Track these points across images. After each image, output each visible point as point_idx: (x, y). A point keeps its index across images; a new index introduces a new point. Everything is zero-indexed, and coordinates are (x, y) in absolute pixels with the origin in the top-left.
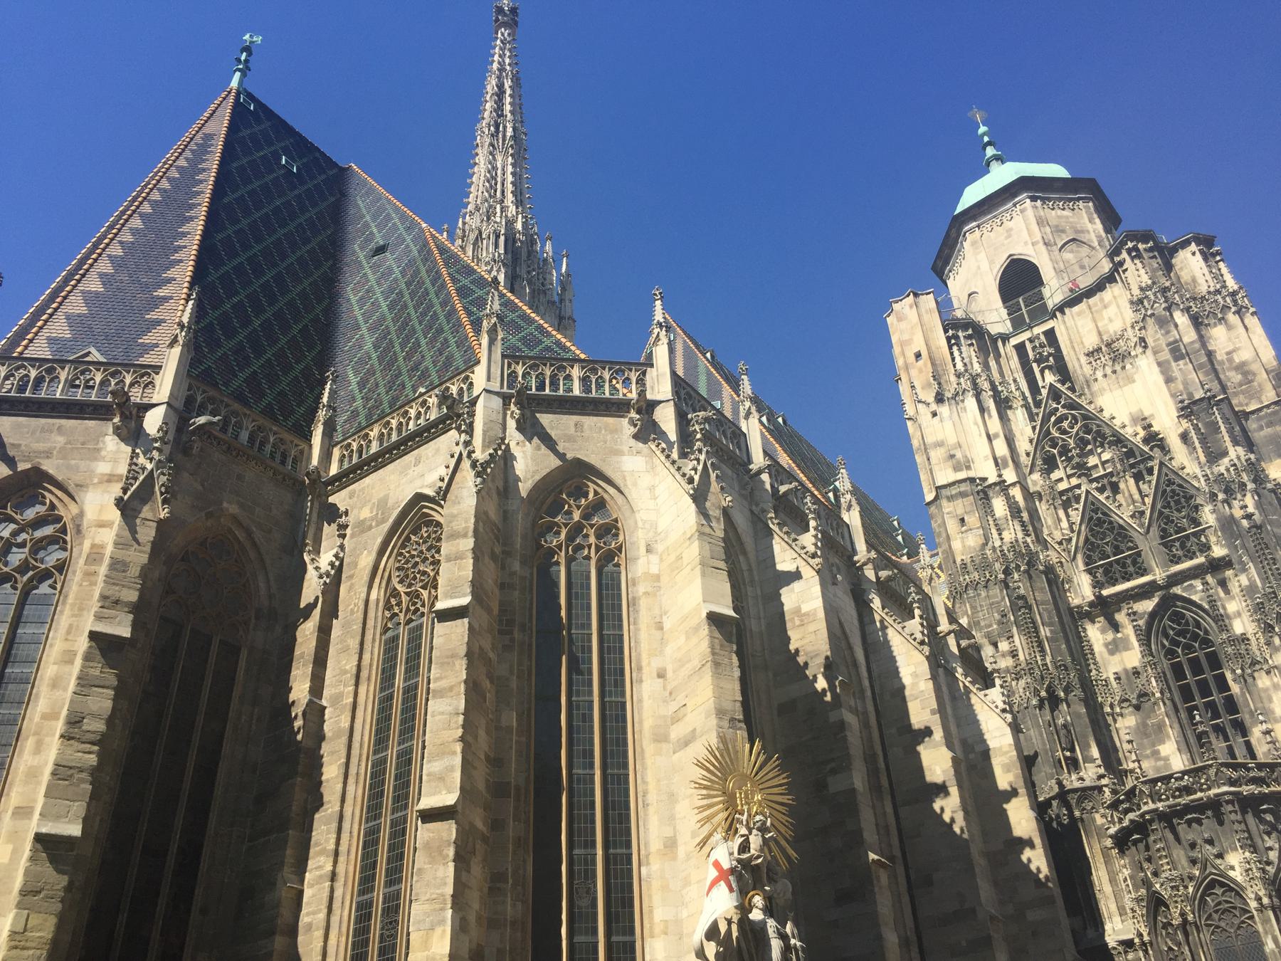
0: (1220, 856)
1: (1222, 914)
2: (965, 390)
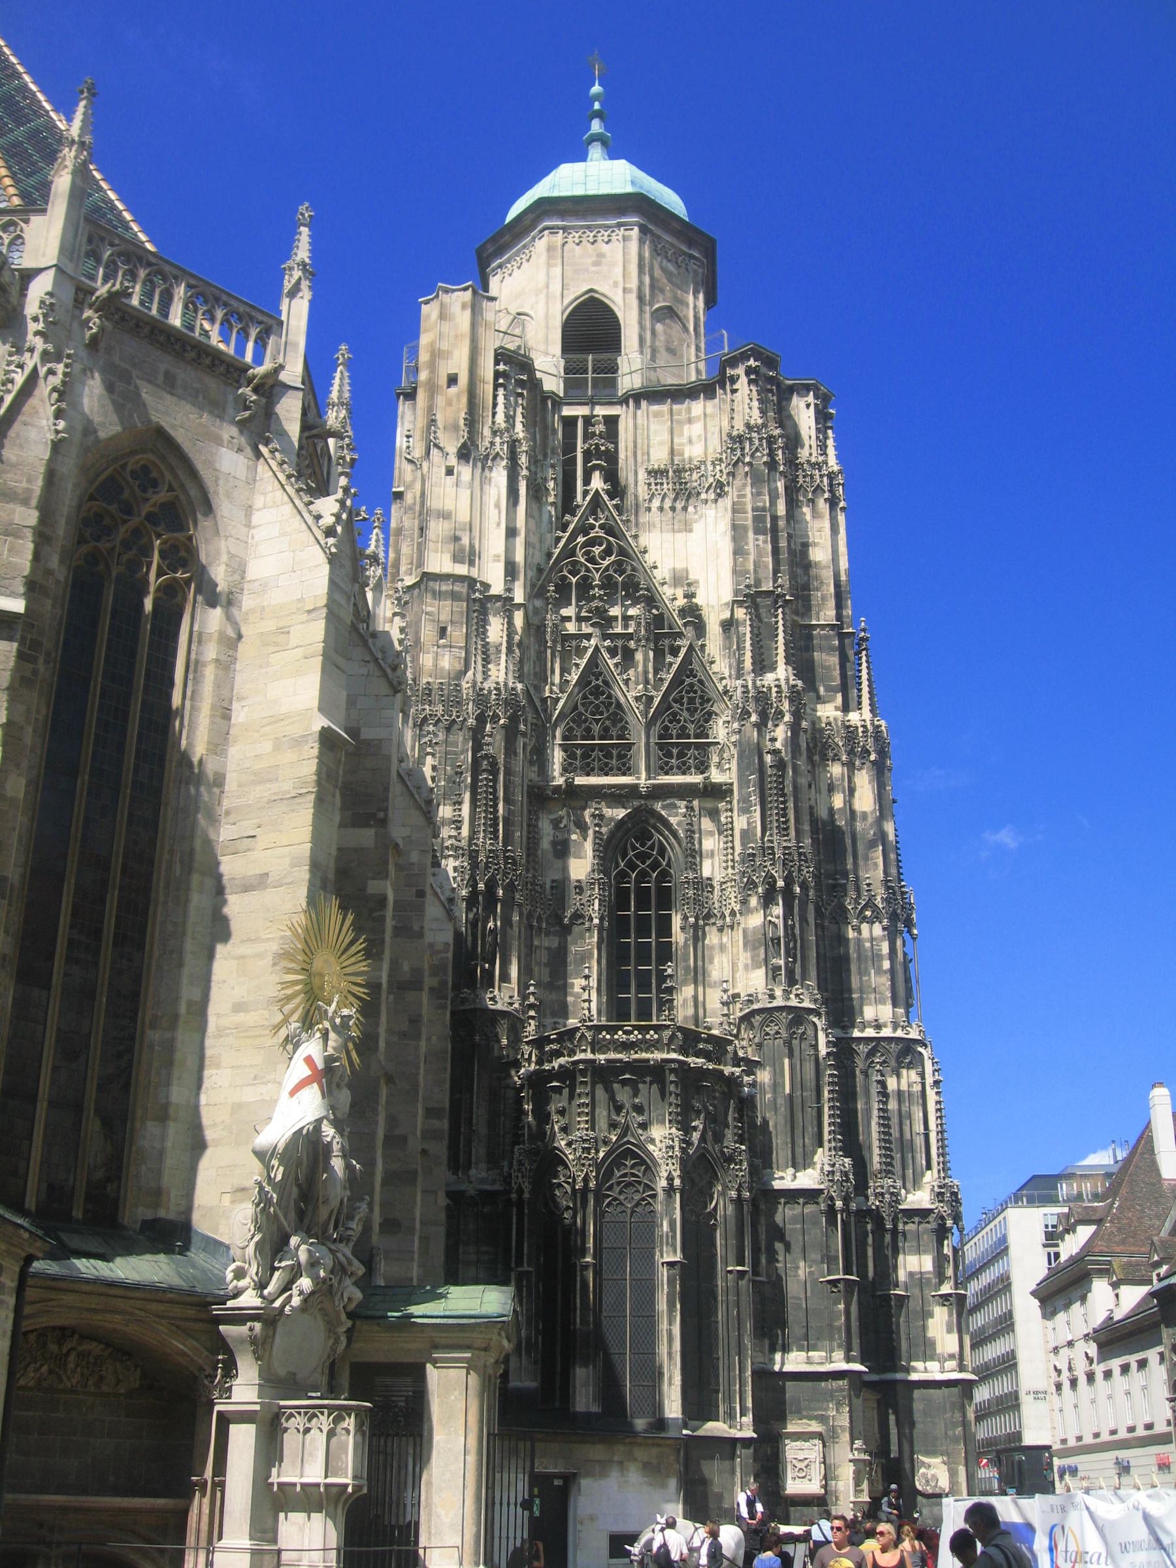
0: (644, 1126)
1: (625, 1187)
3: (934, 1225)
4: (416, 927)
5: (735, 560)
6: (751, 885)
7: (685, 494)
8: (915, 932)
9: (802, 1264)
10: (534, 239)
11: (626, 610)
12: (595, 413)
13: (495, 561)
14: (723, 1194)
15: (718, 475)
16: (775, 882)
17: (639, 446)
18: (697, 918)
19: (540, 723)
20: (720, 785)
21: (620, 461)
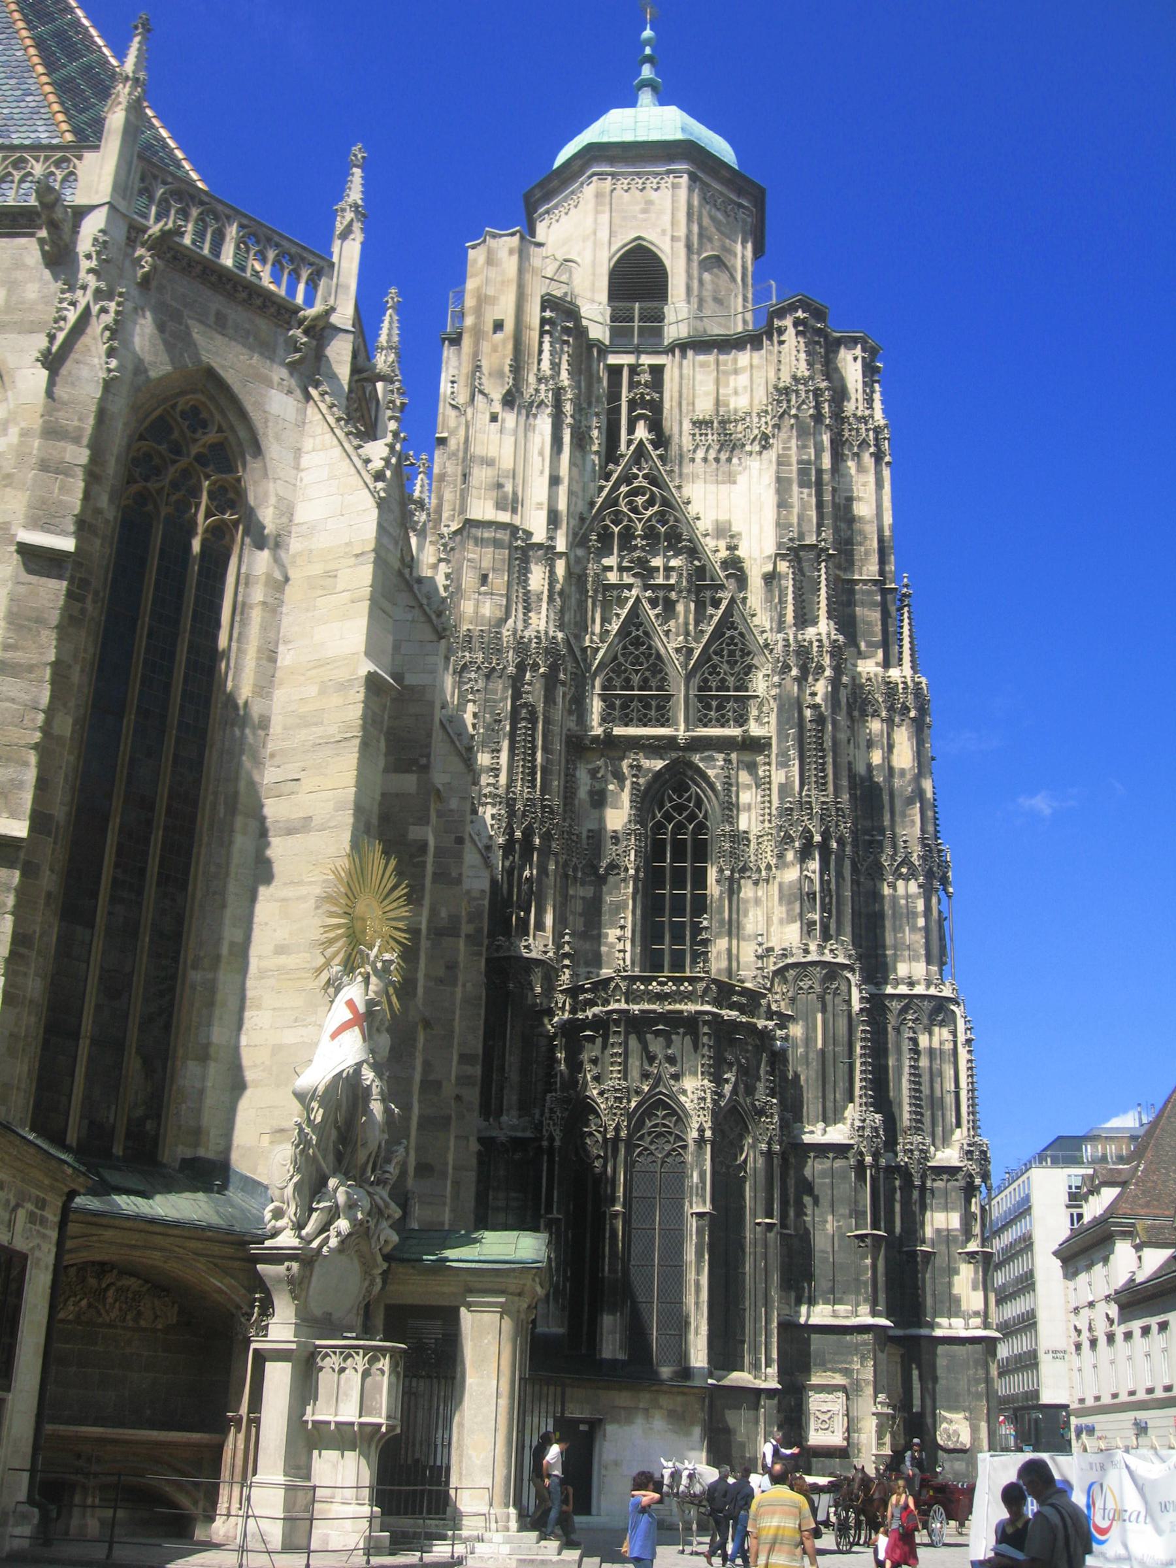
0: (676, 1077)
1: (656, 1137)
2: (542, 402)
3: (962, 1183)
4: (454, 874)
5: (779, 513)
6: (788, 839)
7: (730, 445)
8: (951, 890)
9: (830, 1218)
10: (582, 184)
11: (668, 561)
12: (641, 362)
14: (753, 1146)
15: (762, 429)
16: (812, 837)
17: (684, 396)
18: (732, 871)
20: (759, 738)
21: (665, 412)
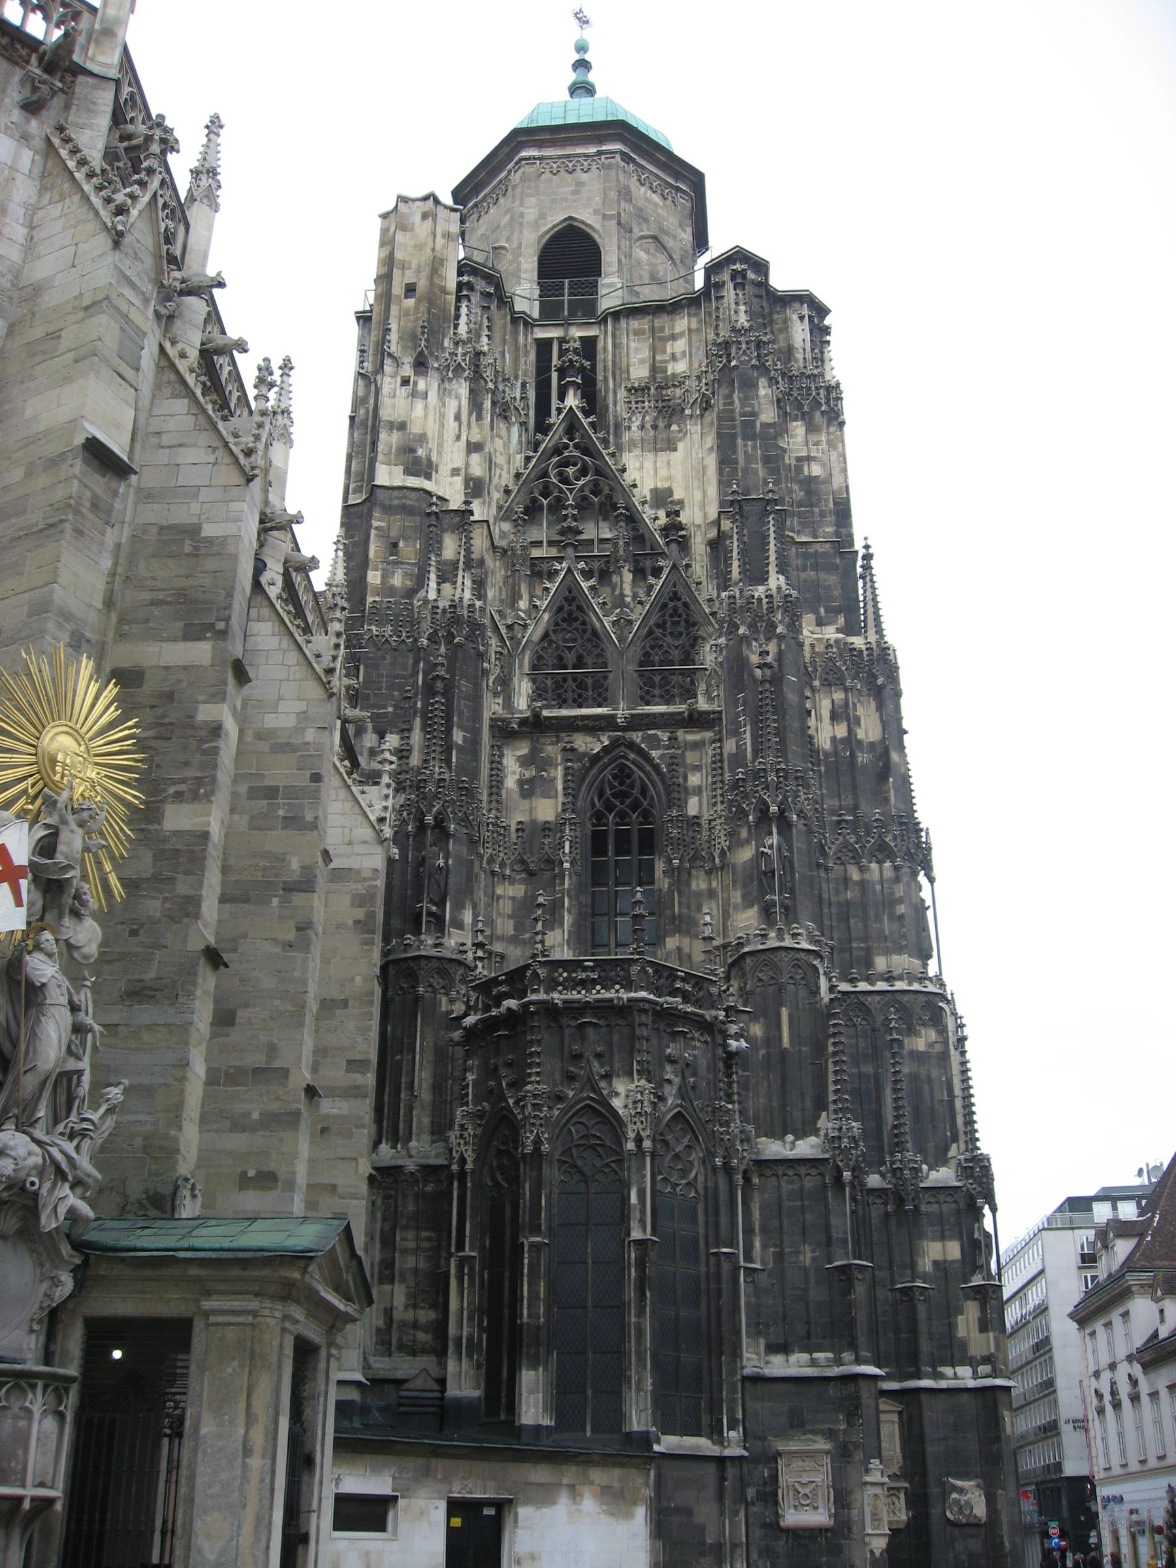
0: (608, 1077)
4: (309, 817)
7: (670, 412)
10: (510, 171)
13: (453, 475)
19: (505, 652)
20: (708, 713)
